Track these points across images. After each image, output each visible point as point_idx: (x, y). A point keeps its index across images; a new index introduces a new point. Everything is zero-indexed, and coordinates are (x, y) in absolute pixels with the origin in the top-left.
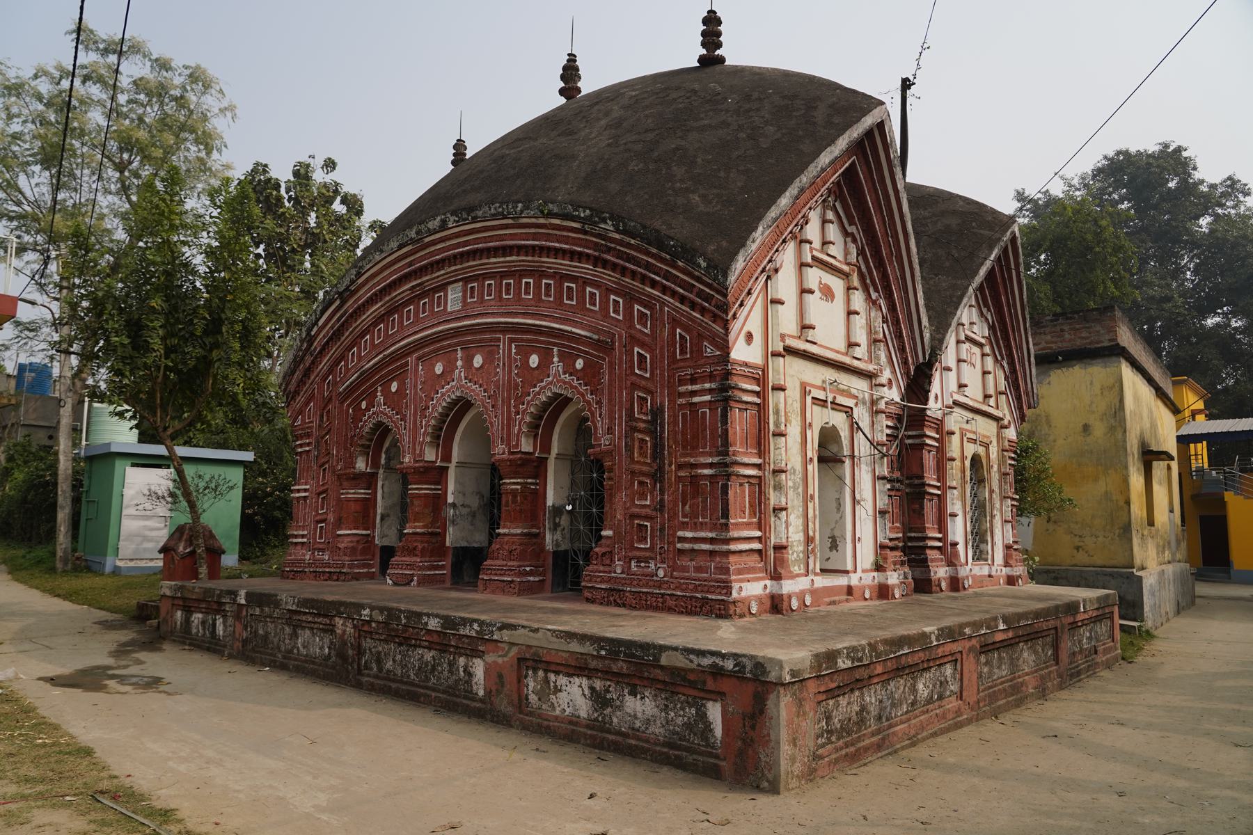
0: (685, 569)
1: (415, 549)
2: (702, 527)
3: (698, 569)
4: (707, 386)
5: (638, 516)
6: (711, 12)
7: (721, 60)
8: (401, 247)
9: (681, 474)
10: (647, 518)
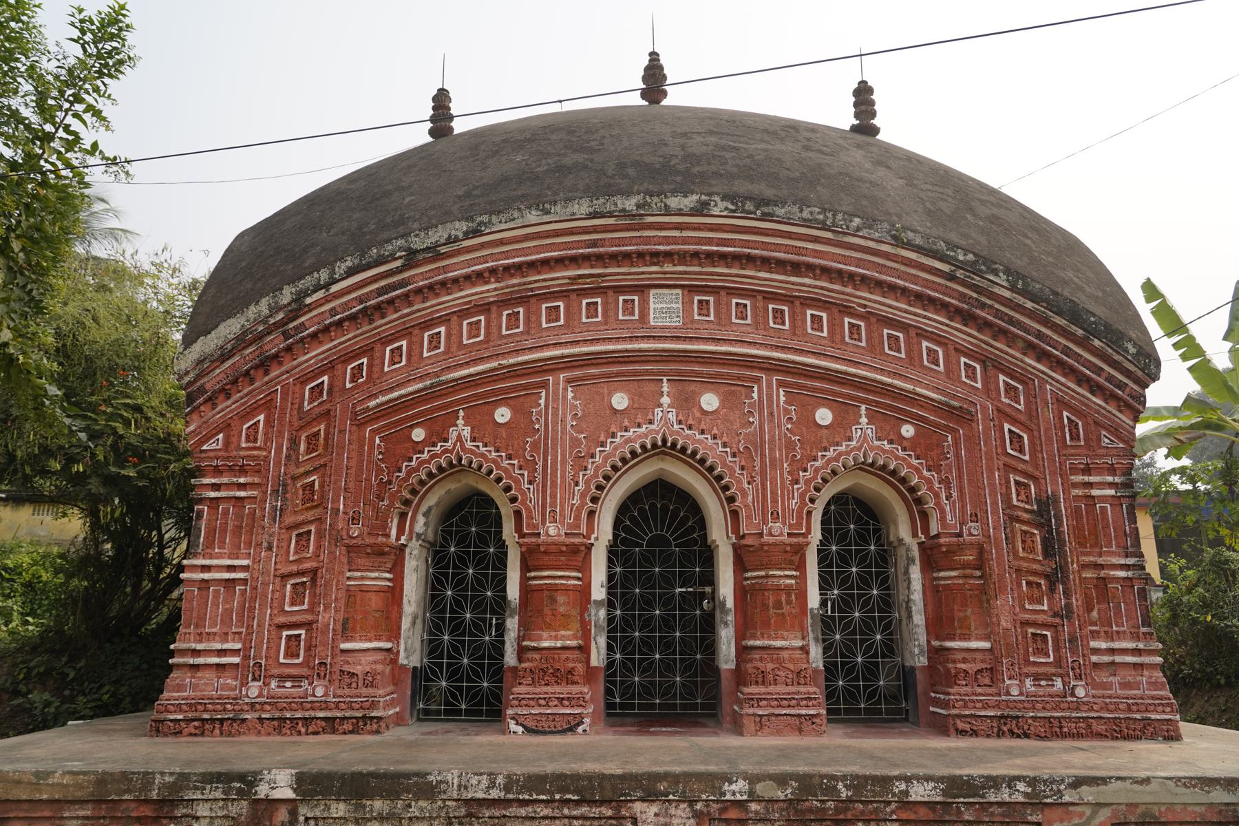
0: (1104, 686)
1: (571, 672)
2: (1119, 635)
3: (1125, 685)
4: (1110, 479)
5: (1034, 624)
6: (863, 83)
7: (875, 131)
8: (593, 215)
9: (1088, 574)
10: (1044, 625)
